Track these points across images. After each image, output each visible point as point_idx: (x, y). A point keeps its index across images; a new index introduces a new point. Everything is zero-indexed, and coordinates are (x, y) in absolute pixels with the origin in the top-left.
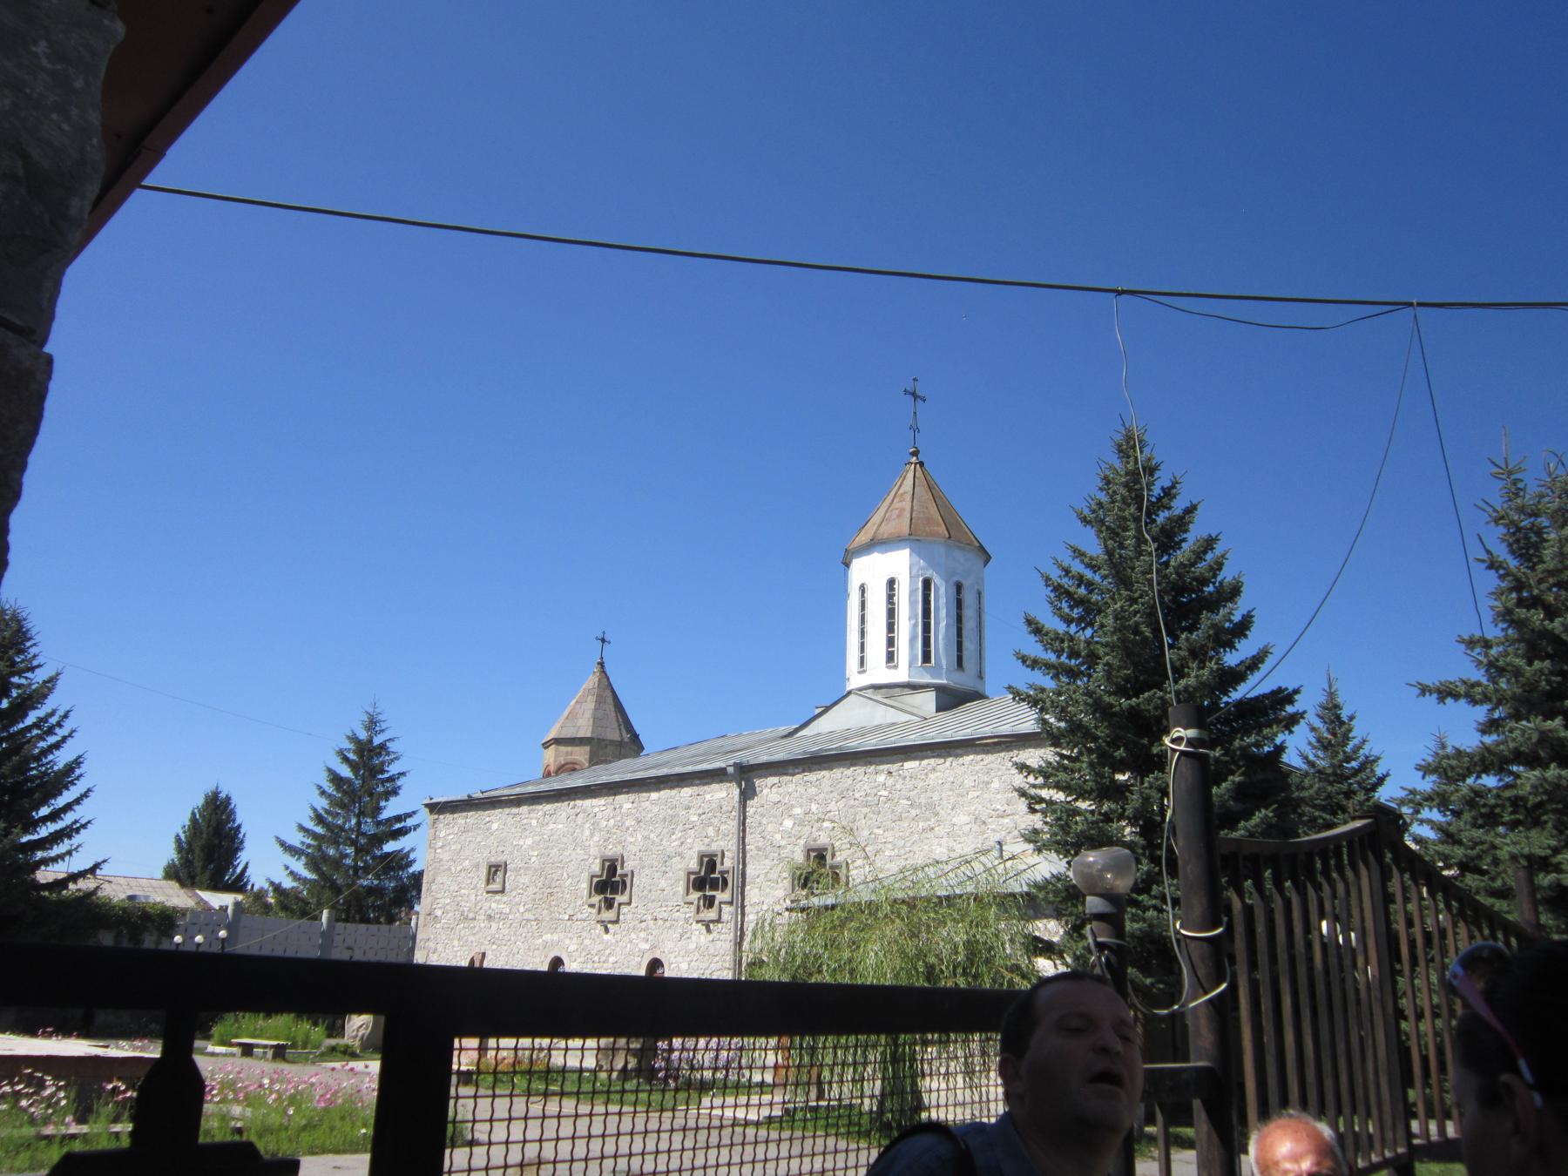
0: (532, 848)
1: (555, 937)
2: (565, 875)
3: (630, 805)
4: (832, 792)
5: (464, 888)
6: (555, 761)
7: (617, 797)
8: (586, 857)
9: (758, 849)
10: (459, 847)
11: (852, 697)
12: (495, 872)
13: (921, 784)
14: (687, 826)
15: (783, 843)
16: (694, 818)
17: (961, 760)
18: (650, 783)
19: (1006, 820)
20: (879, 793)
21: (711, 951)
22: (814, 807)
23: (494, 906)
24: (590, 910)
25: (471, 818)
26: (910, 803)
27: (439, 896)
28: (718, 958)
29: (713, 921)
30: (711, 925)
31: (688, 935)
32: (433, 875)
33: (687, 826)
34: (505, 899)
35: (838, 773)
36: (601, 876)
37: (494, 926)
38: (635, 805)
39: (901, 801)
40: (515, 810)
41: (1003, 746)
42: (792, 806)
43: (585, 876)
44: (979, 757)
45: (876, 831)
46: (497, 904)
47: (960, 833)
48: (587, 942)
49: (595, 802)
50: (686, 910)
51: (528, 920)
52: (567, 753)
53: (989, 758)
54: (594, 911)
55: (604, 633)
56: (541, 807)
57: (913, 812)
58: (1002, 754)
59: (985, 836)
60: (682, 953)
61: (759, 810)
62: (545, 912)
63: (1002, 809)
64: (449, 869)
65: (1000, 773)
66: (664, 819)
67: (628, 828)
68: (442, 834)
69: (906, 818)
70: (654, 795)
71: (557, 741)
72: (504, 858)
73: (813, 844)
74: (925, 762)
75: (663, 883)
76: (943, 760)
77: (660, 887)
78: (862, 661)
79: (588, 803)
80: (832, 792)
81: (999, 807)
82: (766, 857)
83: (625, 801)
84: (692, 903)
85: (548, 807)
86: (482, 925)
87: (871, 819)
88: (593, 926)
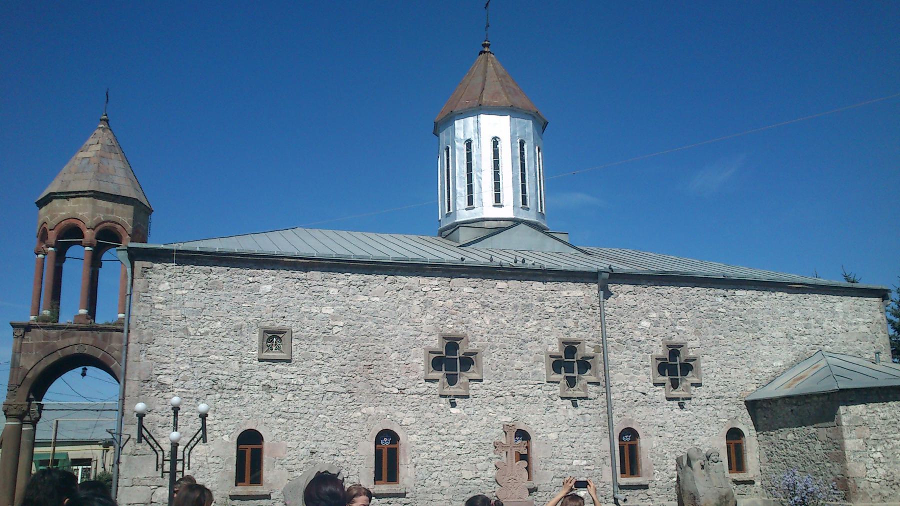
0: (334, 318)
1: (382, 411)
2: (388, 348)
3: (472, 290)
4: (681, 304)
5: (215, 354)
6: (93, 216)
7: (454, 280)
8: (416, 333)
9: (619, 341)
10: (203, 305)
11: (522, 226)
12: (270, 340)
13: (749, 308)
14: (542, 315)
15: (643, 338)
16: (552, 310)
17: (773, 294)
18: (498, 273)
19: (805, 338)
20: (719, 310)
21: (582, 423)
22: (667, 314)
23: (274, 375)
24: (429, 384)
25: (219, 274)
26: (742, 319)
27: (166, 360)
28: (588, 428)
29: (580, 398)
30: (578, 402)
31: (554, 409)
32: (151, 334)
33: (542, 315)
34: (294, 368)
35: (684, 290)
36: (442, 353)
37: (277, 399)
38: (476, 290)
39: (736, 317)
40: (298, 274)
41: (800, 290)
42: (648, 311)
43: (421, 351)
44: (785, 295)
45: (720, 336)
46: (277, 374)
47: (778, 343)
48: (429, 415)
49: (423, 280)
50: (548, 387)
51: (334, 392)
52: (107, 210)
53: (792, 297)
54: (437, 385)
55: (108, 89)
56: (341, 276)
57: (746, 326)
58: (800, 295)
59: (794, 346)
60: (550, 424)
61: (617, 310)
62: (360, 386)
63: (803, 330)
64: (185, 329)
65: (798, 307)
66: (516, 307)
67: (470, 311)
68: (165, 286)
69: (740, 329)
70: (501, 284)
71: (97, 195)
72: (288, 324)
73: (669, 342)
74: (750, 293)
75: (519, 363)
76: (761, 293)
77: (516, 366)
78: (497, 198)
79: (413, 280)
80: (681, 304)
81: (800, 329)
82: (628, 348)
83: (465, 286)
84: (558, 383)
85: (353, 277)
86: (255, 396)
87: (714, 327)
88: (438, 400)
